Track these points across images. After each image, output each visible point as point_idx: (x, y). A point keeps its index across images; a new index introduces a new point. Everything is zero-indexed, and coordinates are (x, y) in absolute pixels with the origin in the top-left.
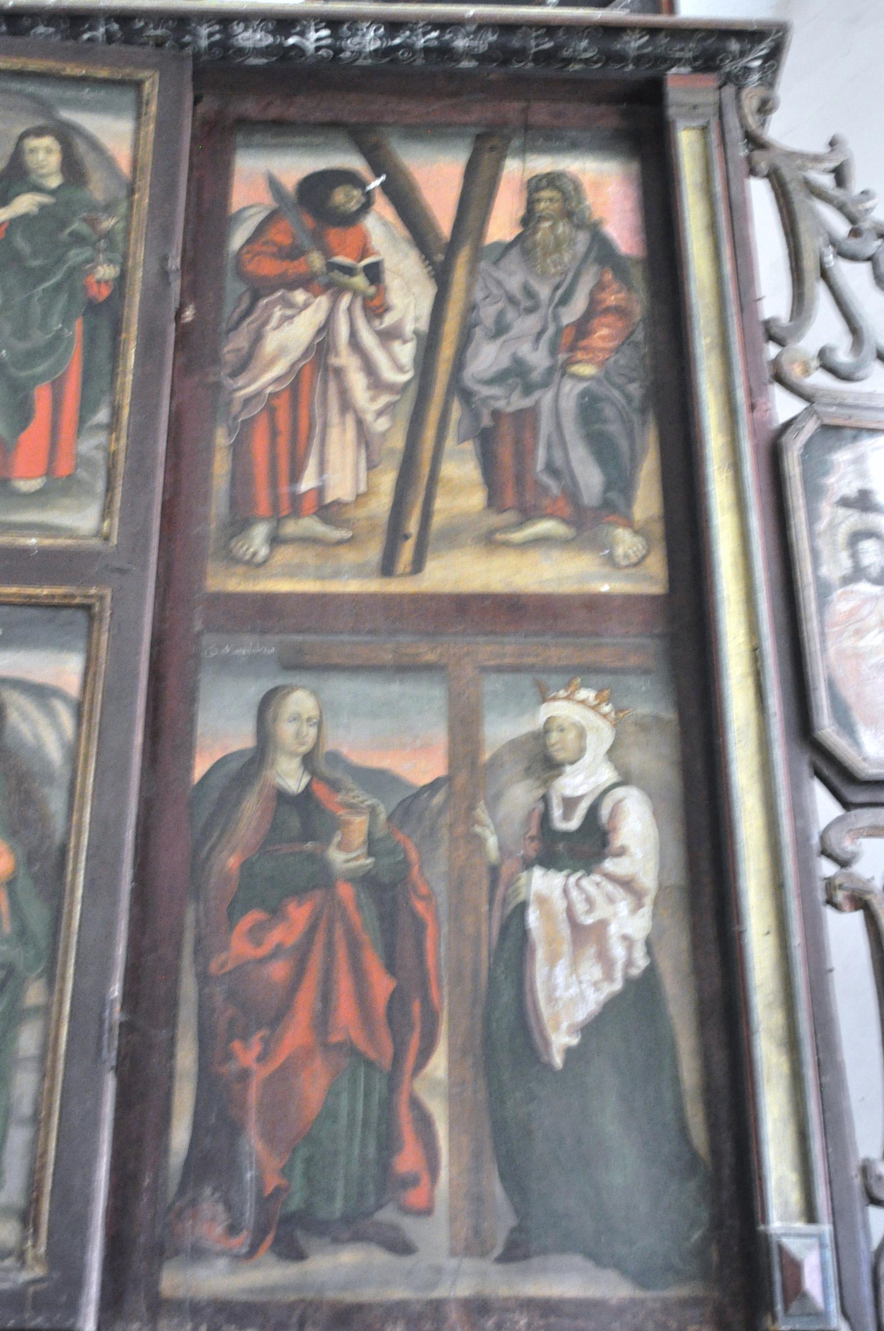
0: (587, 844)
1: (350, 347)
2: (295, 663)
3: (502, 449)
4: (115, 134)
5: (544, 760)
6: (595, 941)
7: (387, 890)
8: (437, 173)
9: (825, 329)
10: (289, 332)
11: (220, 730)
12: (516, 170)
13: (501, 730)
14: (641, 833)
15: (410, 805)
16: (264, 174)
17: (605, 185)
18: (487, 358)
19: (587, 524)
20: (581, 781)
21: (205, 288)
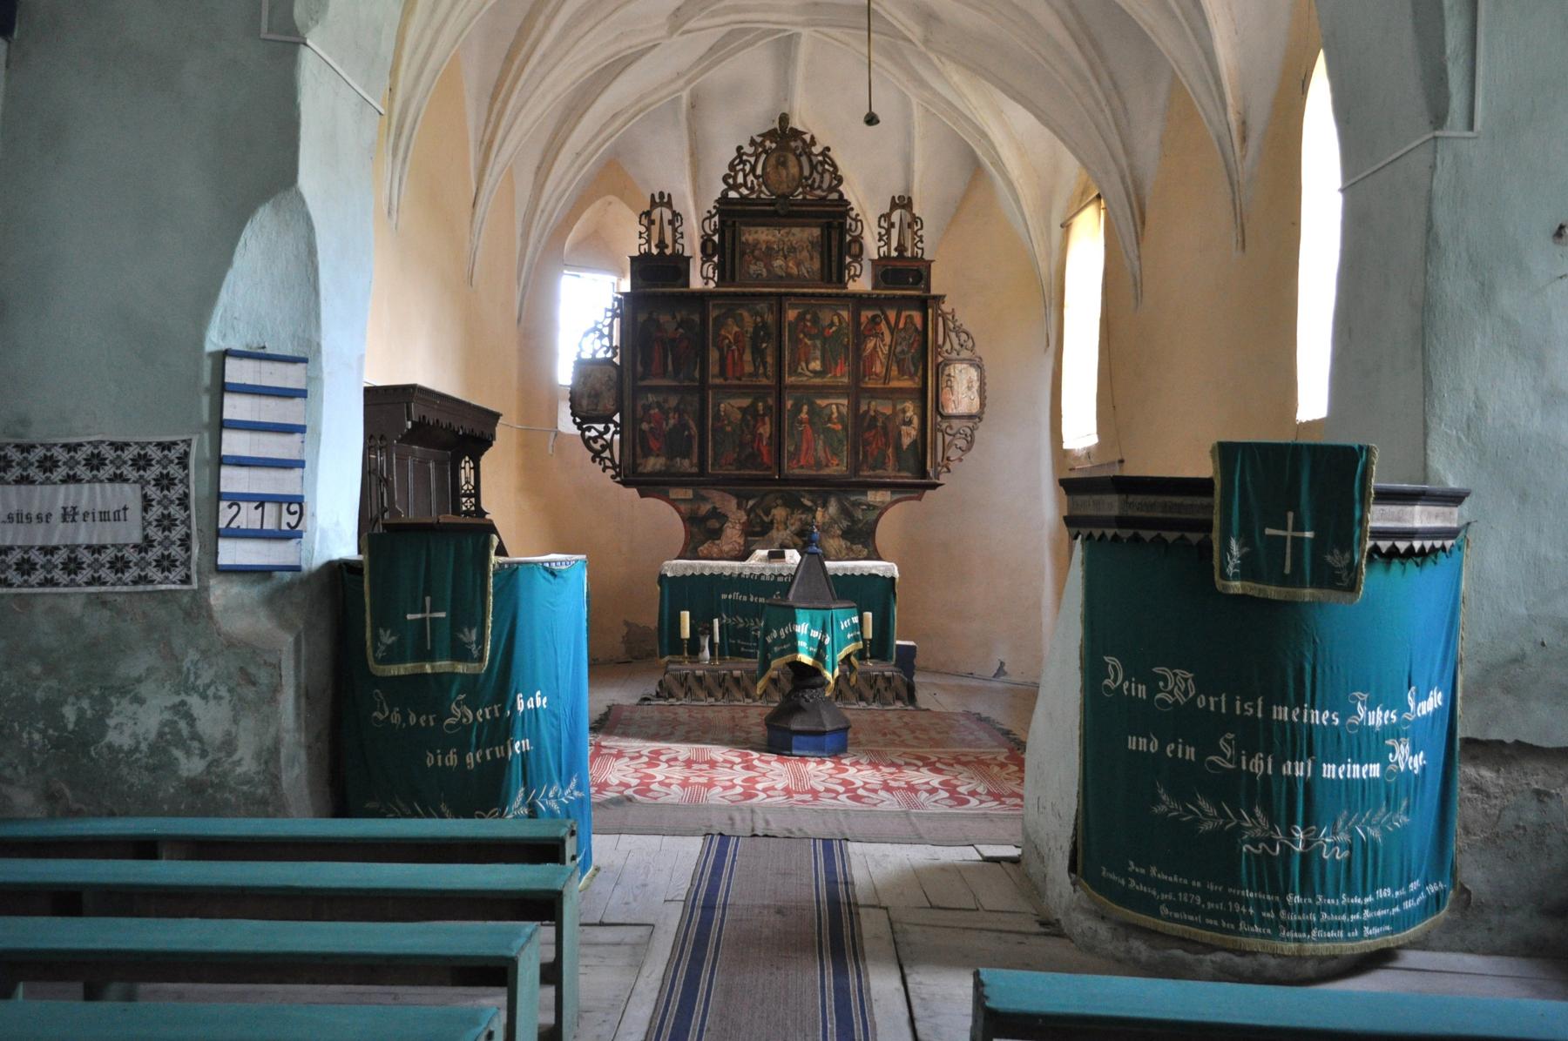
0: (910, 423)
1: (879, 346)
2: (873, 398)
3: (900, 363)
4: (845, 314)
5: (904, 411)
6: (909, 435)
7: (885, 428)
8: (892, 315)
9: (948, 346)
10: (870, 345)
11: (864, 408)
12: (904, 314)
13: (899, 407)
14: (916, 421)
15: (888, 417)
16: (866, 314)
17: (917, 316)
18: (899, 349)
19: (912, 376)
20: (909, 414)
21: (860, 337)
